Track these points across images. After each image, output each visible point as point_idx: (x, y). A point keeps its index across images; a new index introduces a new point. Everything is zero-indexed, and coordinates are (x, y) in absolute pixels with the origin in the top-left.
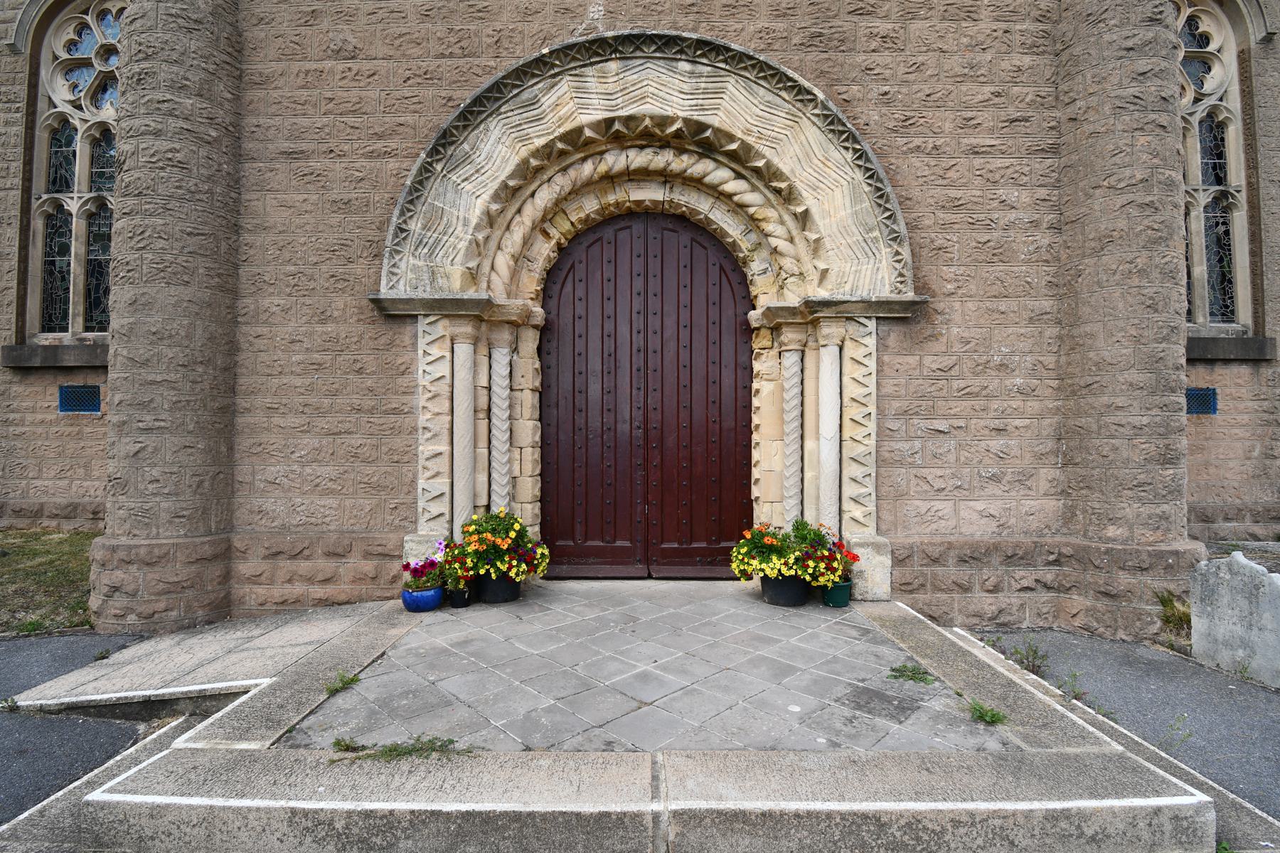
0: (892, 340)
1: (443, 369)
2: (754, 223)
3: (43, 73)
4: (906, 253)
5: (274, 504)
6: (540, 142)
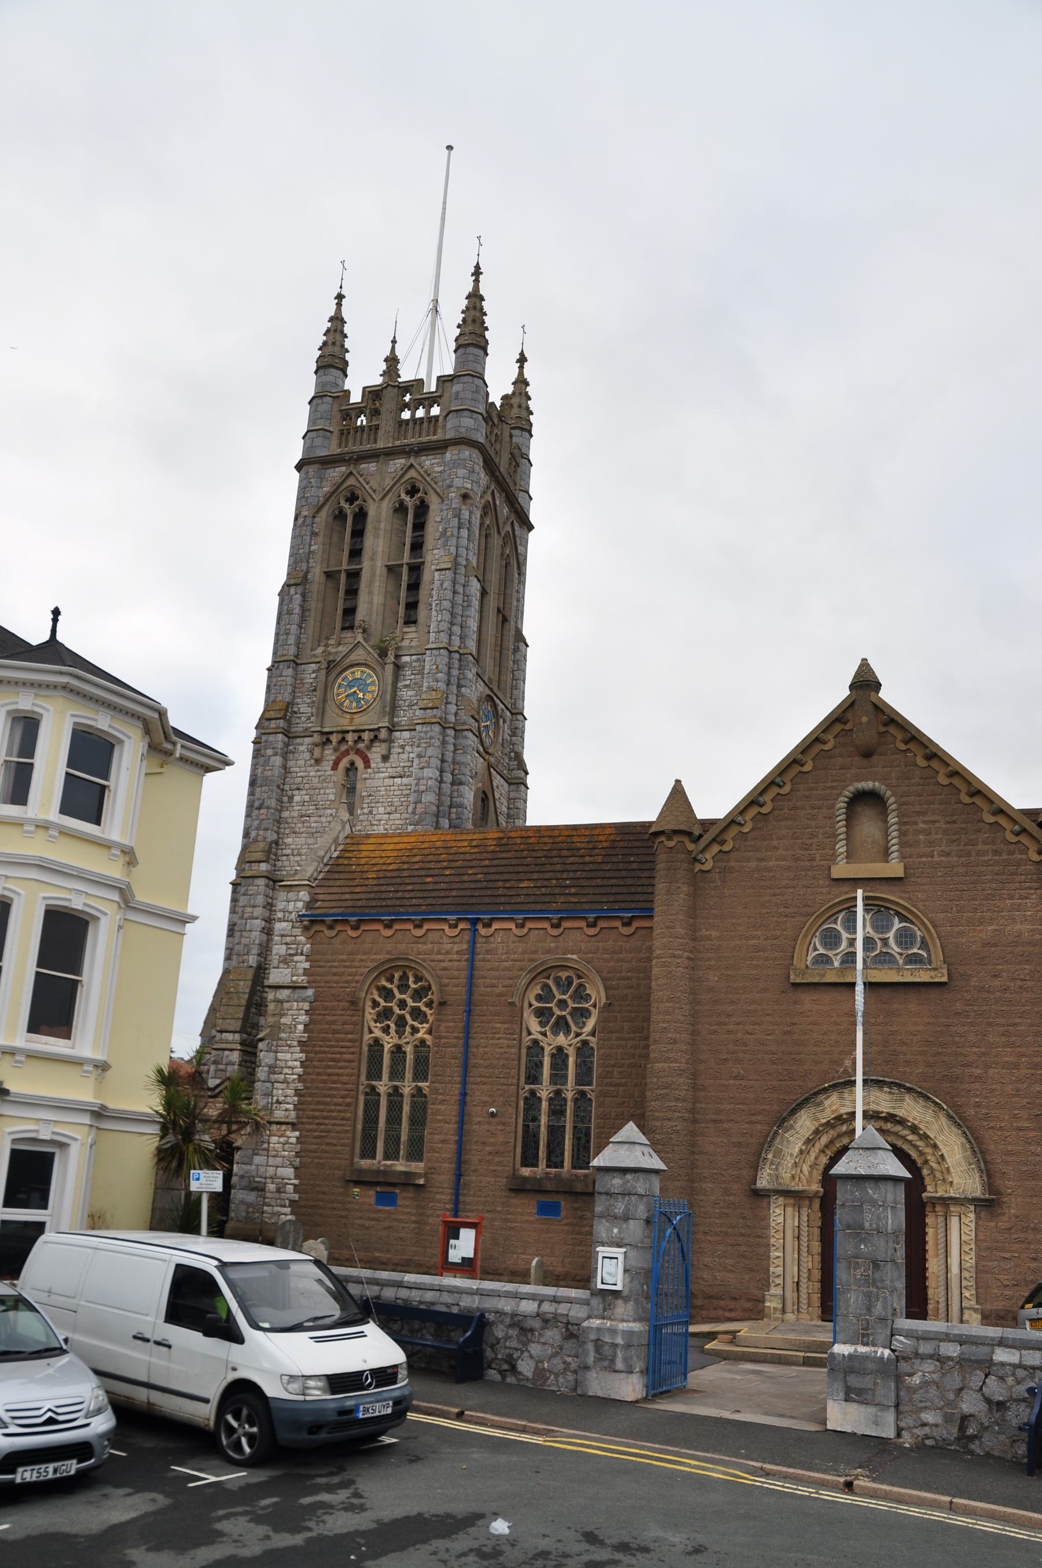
0: (983, 1214)
1: (781, 1219)
2: (922, 1153)
3: (525, 1015)
4: (985, 1178)
6: (824, 1121)
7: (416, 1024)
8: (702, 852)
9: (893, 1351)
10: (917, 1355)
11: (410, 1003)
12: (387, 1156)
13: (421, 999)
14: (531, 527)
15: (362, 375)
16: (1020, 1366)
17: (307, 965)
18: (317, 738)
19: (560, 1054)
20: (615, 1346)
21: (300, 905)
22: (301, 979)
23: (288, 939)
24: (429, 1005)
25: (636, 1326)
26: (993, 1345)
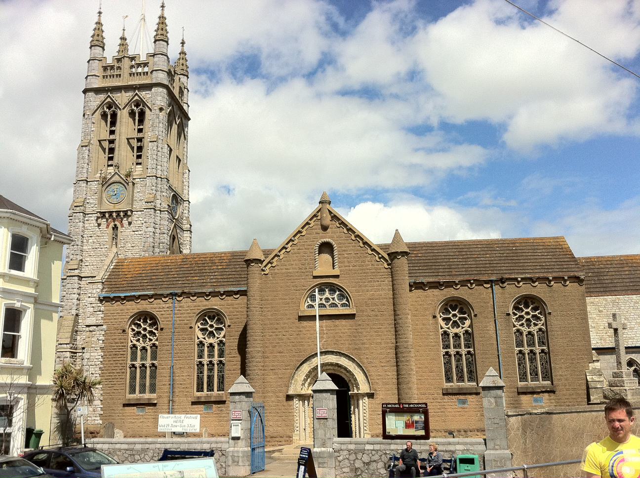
5: (271, 429)
6: (312, 367)
7: (151, 338)
8: (265, 267)
9: (333, 449)
10: (341, 450)
11: (148, 329)
12: (140, 393)
13: (153, 327)
14: (189, 119)
15: (111, 52)
16: (373, 450)
17: (103, 316)
18: (99, 215)
19: (211, 346)
20: (239, 457)
21: (98, 290)
22: (100, 322)
23: (93, 305)
24: (157, 329)
25: (246, 449)
26: (365, 444)
